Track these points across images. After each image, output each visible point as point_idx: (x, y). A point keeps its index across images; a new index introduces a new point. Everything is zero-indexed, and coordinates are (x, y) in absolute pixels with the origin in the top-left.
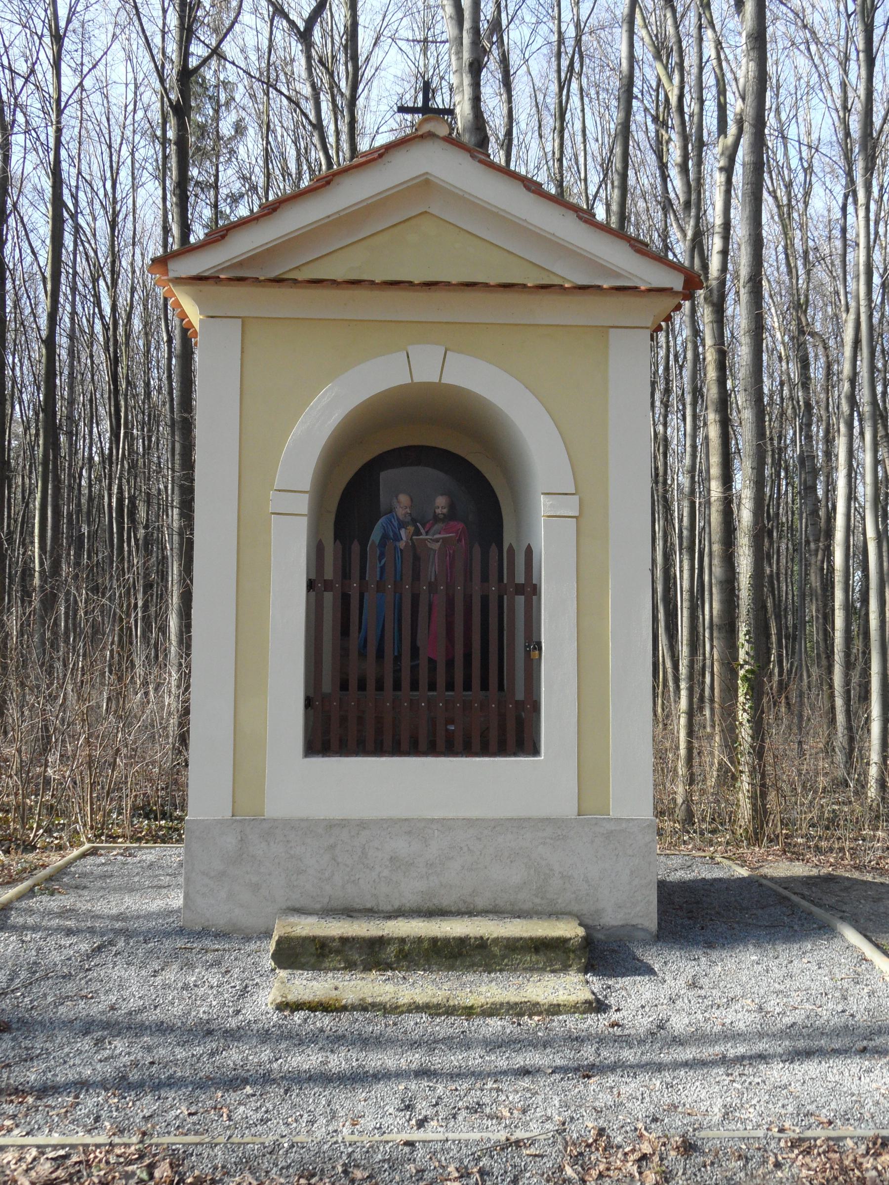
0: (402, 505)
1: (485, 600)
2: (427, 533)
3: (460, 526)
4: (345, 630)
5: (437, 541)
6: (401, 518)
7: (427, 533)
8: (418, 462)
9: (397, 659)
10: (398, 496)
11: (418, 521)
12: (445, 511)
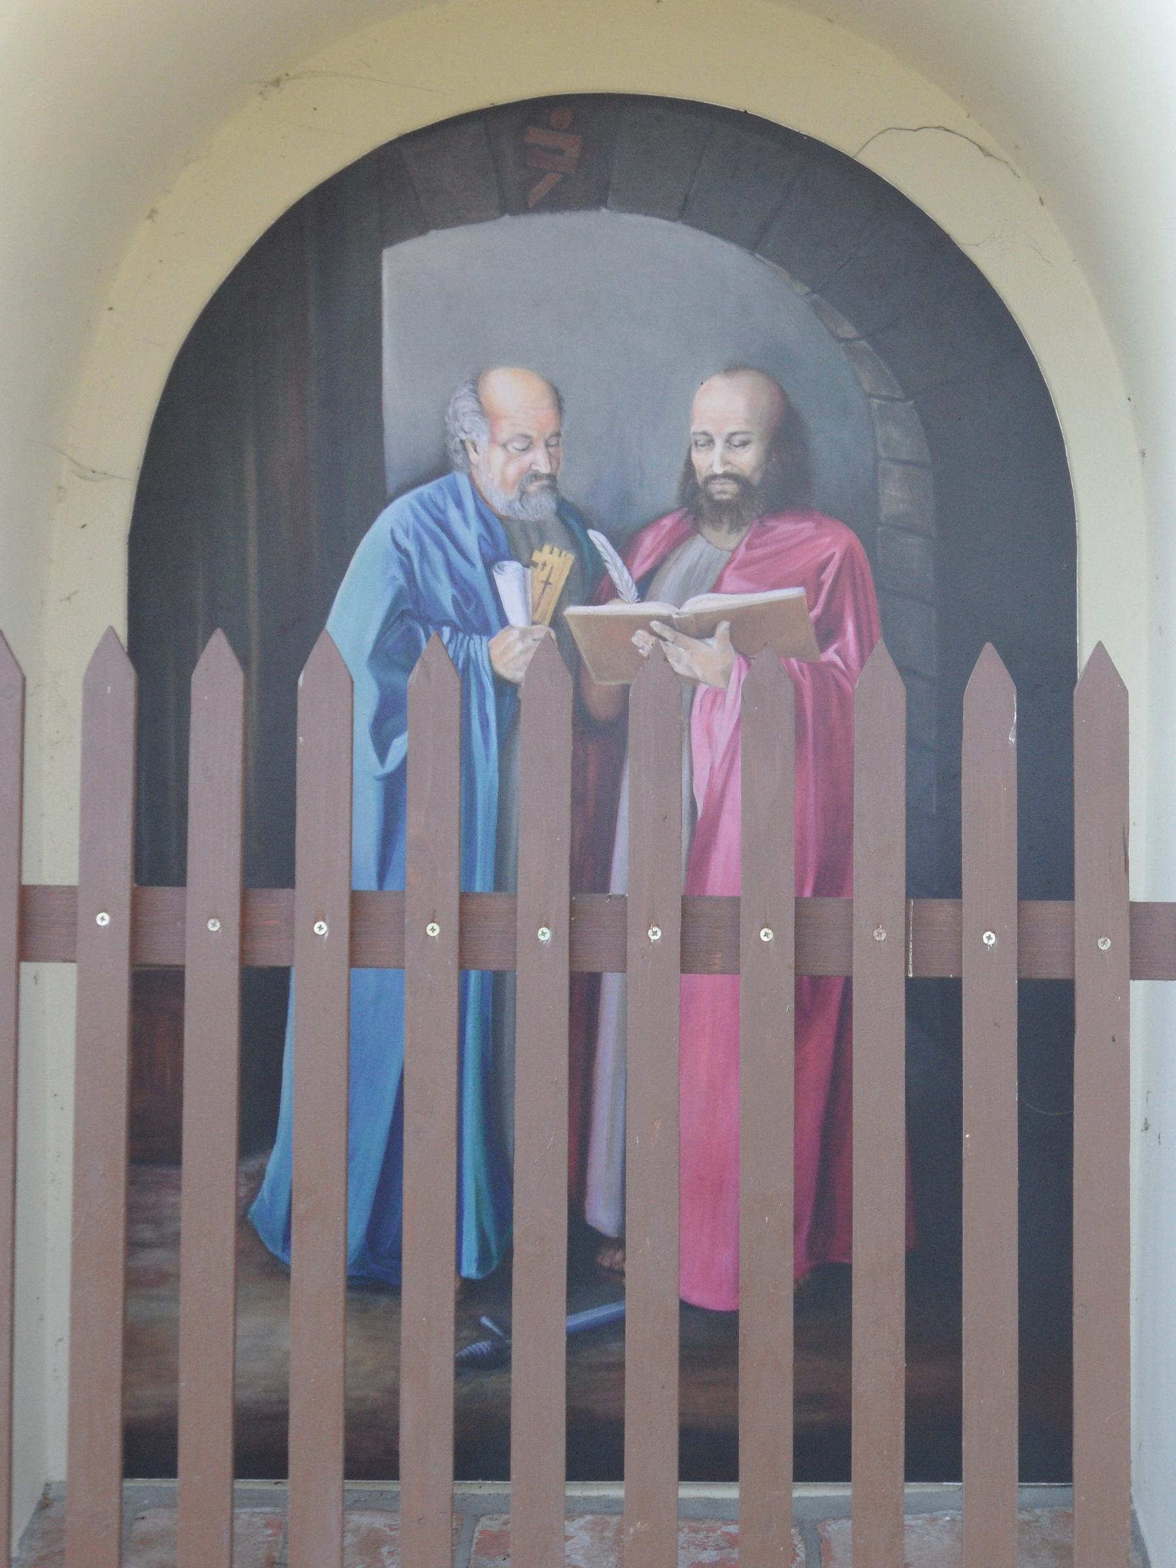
0: (506, 432)
1: (934, 1008)
2: (644, 588)
3: (830, 544)
4: (153, 1139)
5: (702, 628)
6: (500, 500)
7: (644, 588)
8: (588, 189)
9: (485, 1293)
10: (500, 378)
11: (593, 524)
12: (747, 460)
